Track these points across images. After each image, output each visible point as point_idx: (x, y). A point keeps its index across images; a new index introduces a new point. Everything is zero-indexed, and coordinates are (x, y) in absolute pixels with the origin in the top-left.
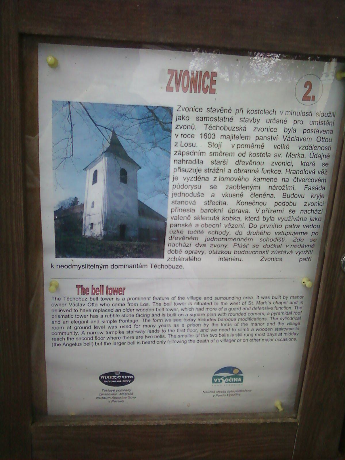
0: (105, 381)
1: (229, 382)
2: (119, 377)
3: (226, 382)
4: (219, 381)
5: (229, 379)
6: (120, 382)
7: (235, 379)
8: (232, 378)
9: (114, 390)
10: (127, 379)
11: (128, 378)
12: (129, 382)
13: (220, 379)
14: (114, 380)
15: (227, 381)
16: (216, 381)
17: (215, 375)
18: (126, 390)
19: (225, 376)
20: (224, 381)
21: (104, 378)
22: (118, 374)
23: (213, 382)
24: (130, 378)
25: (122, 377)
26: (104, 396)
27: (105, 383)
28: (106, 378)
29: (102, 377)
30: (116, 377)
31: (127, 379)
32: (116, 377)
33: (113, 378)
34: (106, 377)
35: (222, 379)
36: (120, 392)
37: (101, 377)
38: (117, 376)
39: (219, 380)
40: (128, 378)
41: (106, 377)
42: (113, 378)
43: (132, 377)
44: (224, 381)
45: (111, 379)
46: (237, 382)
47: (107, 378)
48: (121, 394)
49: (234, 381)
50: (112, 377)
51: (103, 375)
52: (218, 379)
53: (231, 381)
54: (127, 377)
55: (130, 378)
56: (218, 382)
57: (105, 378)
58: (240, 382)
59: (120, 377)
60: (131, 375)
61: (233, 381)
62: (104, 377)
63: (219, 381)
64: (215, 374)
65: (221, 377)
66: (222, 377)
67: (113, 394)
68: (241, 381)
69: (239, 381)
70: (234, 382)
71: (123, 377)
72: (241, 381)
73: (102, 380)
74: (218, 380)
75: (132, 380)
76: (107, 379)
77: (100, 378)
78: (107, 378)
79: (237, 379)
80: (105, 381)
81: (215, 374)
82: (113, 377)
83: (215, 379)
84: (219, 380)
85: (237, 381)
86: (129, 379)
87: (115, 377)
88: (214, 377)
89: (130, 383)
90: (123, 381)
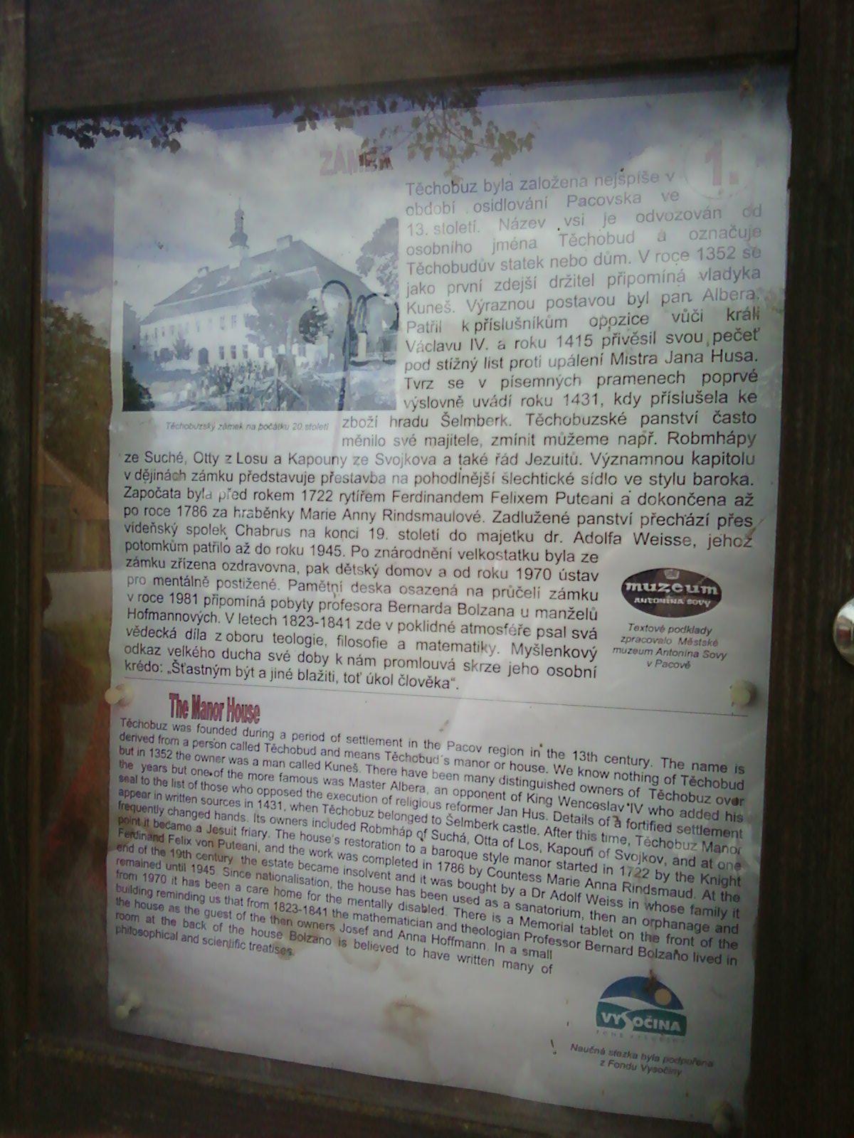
0: (637, 600)
1: (643, 1029)
2: (677, 589)
3: (636, 1029)
4: (617, 1022)
5: (644, 1020)
6: (681, 604)
7: (661, 1022)
8: (653, 1018)
9: (662, 629)
10: (700, 595)
11: (704, 592)
12: (707, 606)
13: (619, 1016)
14: (662, 595)
15: (637, 1025)
16: (607, 1020)
17: (603, 1000)
18: (698, 631)
19: (633, 1010)
20: (630, 1024)
21: (634, 589)
22: (673, 578)
23: (600, 1022)
24: (709, 592)
25: (685, 588)
26: (634, 645)
27: (641, 607)
28: (640, 589)
29: (629, 585)
30: (667, 585)
31: (700, 595)
32: (667, 585)
33: (659, 588)
34: (639, 585)
35: (624, 1015)
36: (680, 635)
37: (626, 586)
38: (672, 582)
39: (617, 1019)
40: (704, 592)
41: (639, 585)
42: (659, 590)
43: (715, 589)
44: (630, 1024)
45: (654, 592)
46: (669, 1032)
47: (642, 587)
48: (683, 640)
49: (661, 1028)
50: (658, 588)
51: (630, 579)
52: (614, 1015)
53: (650, 1027)
54: (700, 589)
55: (709, 592)
56: (612, 1024)
57: (637, 587)
58: (675, 1033)
59: (681, 587)
60: (709, 582)
61: (655, 1027)
62: (634, 585)
63: (617, 1022)
64: (602, 998)
65: (620, 1010)
66: (627, 1010)
67: (661, 641)
68: (679, 1029)
69: (673, 1029)
70: (657, 1031)
71: (688, 587)
72: (679, 1029)
73: (629, 595)
74: (612, 1017)
75: (716, 598)
76: (644, 594)
77: (624, 587)
78: (642, 587)
79: (668, 1022)
80: (637, 600)
81: (602, 998)
82: (660, 585)
83: (604, 1014)
84: (617, 1019)
85: (667, 1029)
86: (706, 596)
87: (667, 588)
88: (603, 1007)
89: (708, 609)
90: (690, 601)
